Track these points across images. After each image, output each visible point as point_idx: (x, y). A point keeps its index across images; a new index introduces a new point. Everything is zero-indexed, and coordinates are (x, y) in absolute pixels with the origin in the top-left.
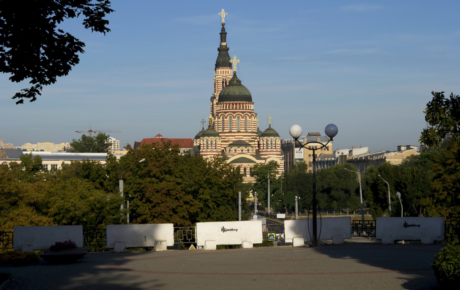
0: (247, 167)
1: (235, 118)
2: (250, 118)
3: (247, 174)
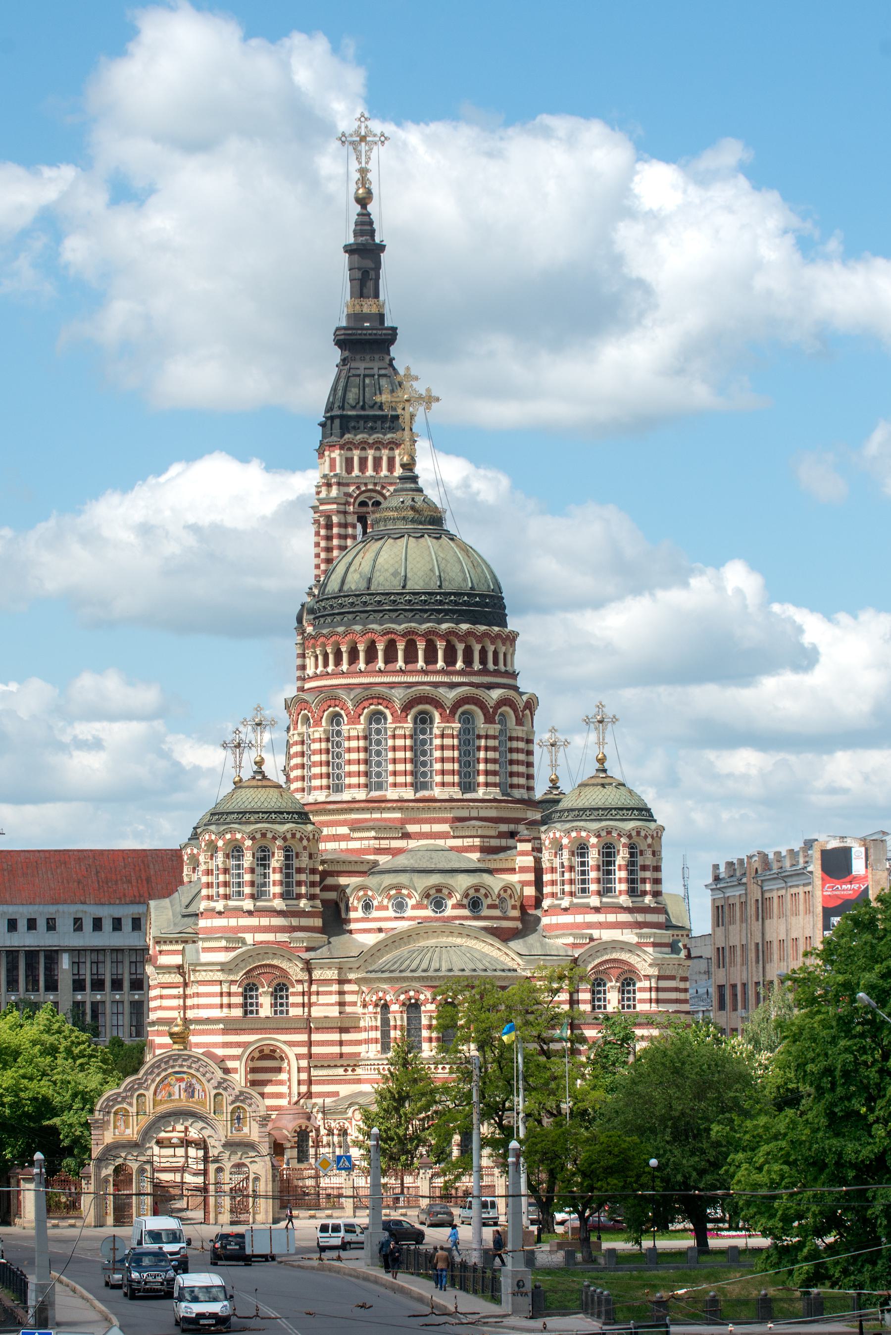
1: (406, 722)
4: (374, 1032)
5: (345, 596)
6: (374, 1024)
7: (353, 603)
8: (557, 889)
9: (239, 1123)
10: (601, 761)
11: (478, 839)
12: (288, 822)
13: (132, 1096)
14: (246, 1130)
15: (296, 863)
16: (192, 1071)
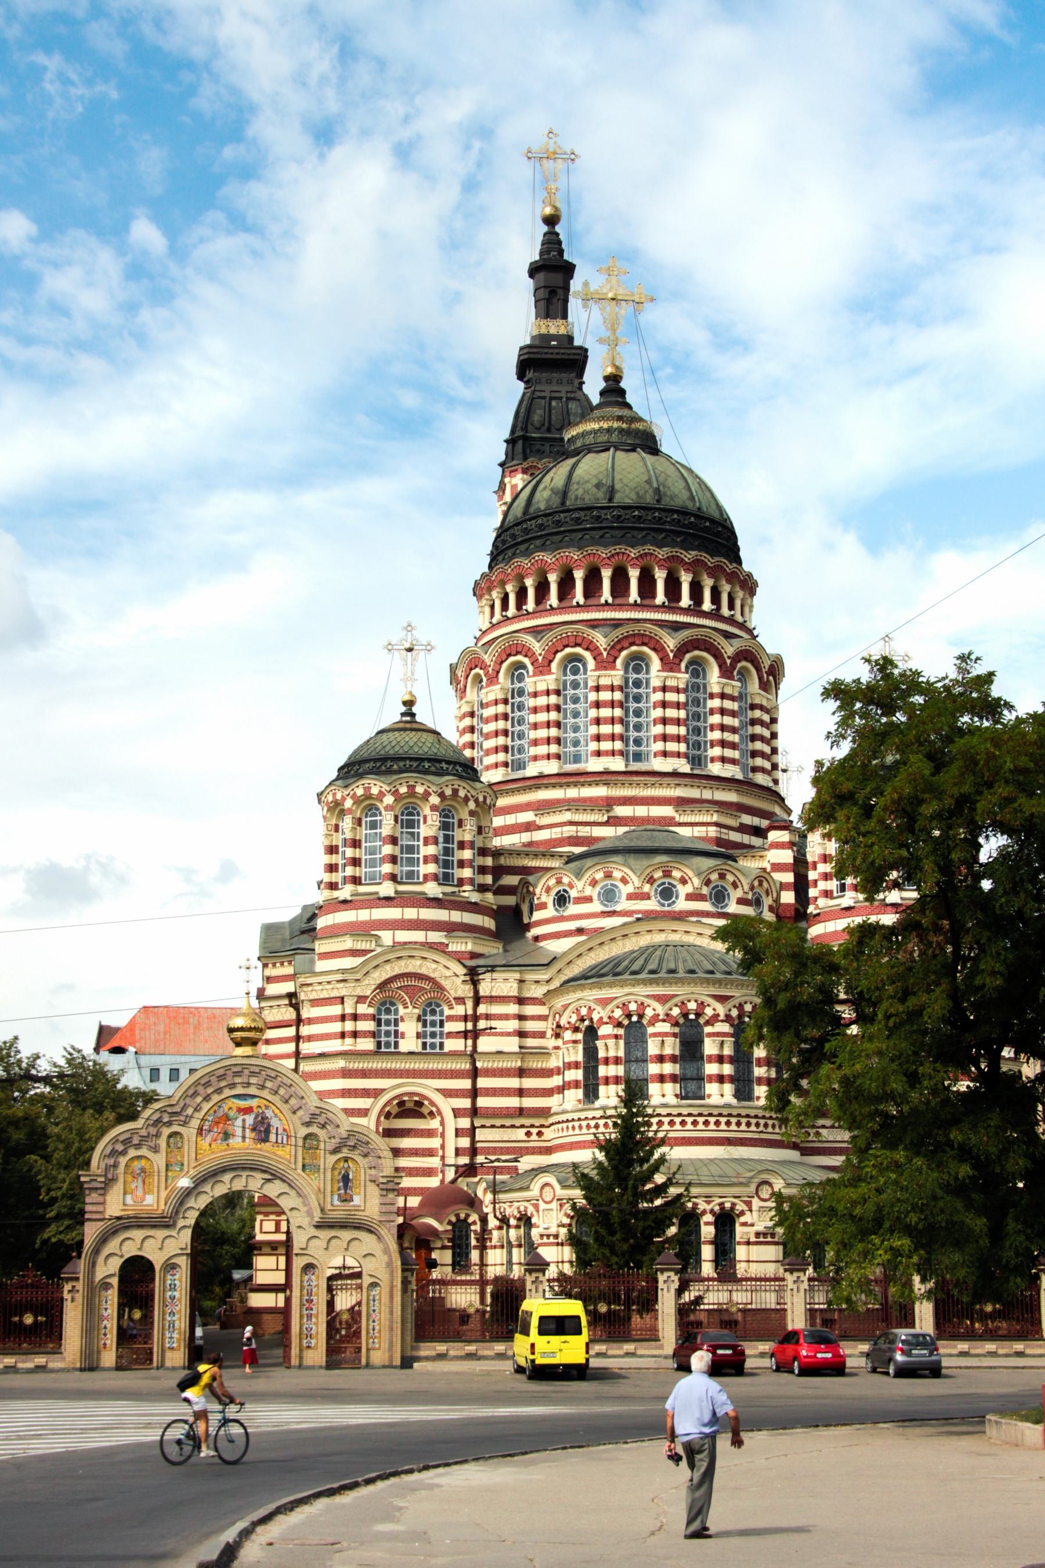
0: (709, 1012)
1: (614, 668)
2: (732, 678)
3: (711, 1079)
4: (573, 1071)
6: (573, 1059)
7: (542, 525)
9: (346, 1187)
11: (714, 828)
12: (448, 774)
13: (158, 1135)
14: (357, 1200)
15: (458, 835)
16: (265, 1094)
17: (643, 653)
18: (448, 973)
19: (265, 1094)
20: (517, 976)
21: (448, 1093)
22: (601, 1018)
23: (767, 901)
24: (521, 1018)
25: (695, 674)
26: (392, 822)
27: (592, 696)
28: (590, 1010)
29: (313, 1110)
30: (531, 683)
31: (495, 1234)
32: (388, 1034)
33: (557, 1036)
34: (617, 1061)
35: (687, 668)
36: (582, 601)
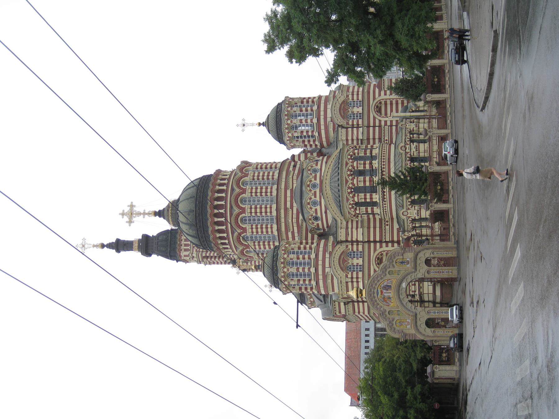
0: (350, 168)
5: (198, 236)
8: (311, 140)
9: (405, 263)
10: (260, 124)
15: (296, 250)
16: (376, 287)
17: (241, 198)
18: (339, 250)
19: (376, 287)
20: (339, 229)
21: (375, 250)
22: (352, 200)
23: (317, 158)
24: (352, 228)
25: (247, 184)
26: (292, 269)
27: (253, 214)
28: (350, 204)
29: (381, 273)
30: (249, 234)
31: (417, 231)
32: (357, 268)
33: (358, 217)
34: (365, 195)
35: (245, 186)
36: (224, 219)
